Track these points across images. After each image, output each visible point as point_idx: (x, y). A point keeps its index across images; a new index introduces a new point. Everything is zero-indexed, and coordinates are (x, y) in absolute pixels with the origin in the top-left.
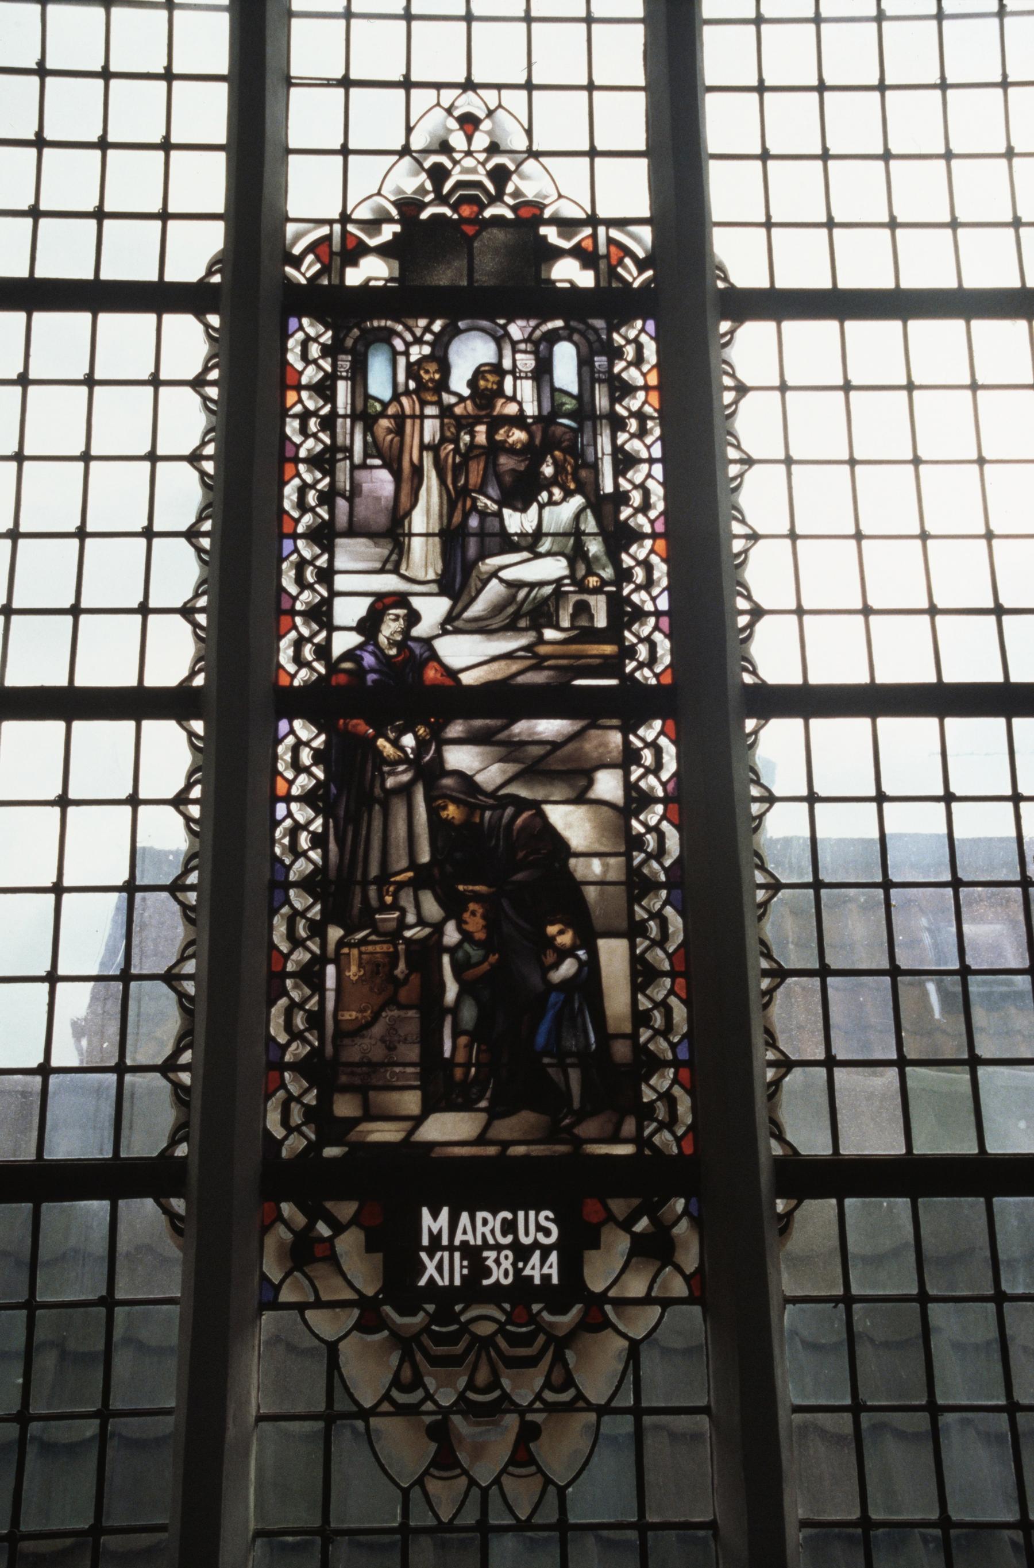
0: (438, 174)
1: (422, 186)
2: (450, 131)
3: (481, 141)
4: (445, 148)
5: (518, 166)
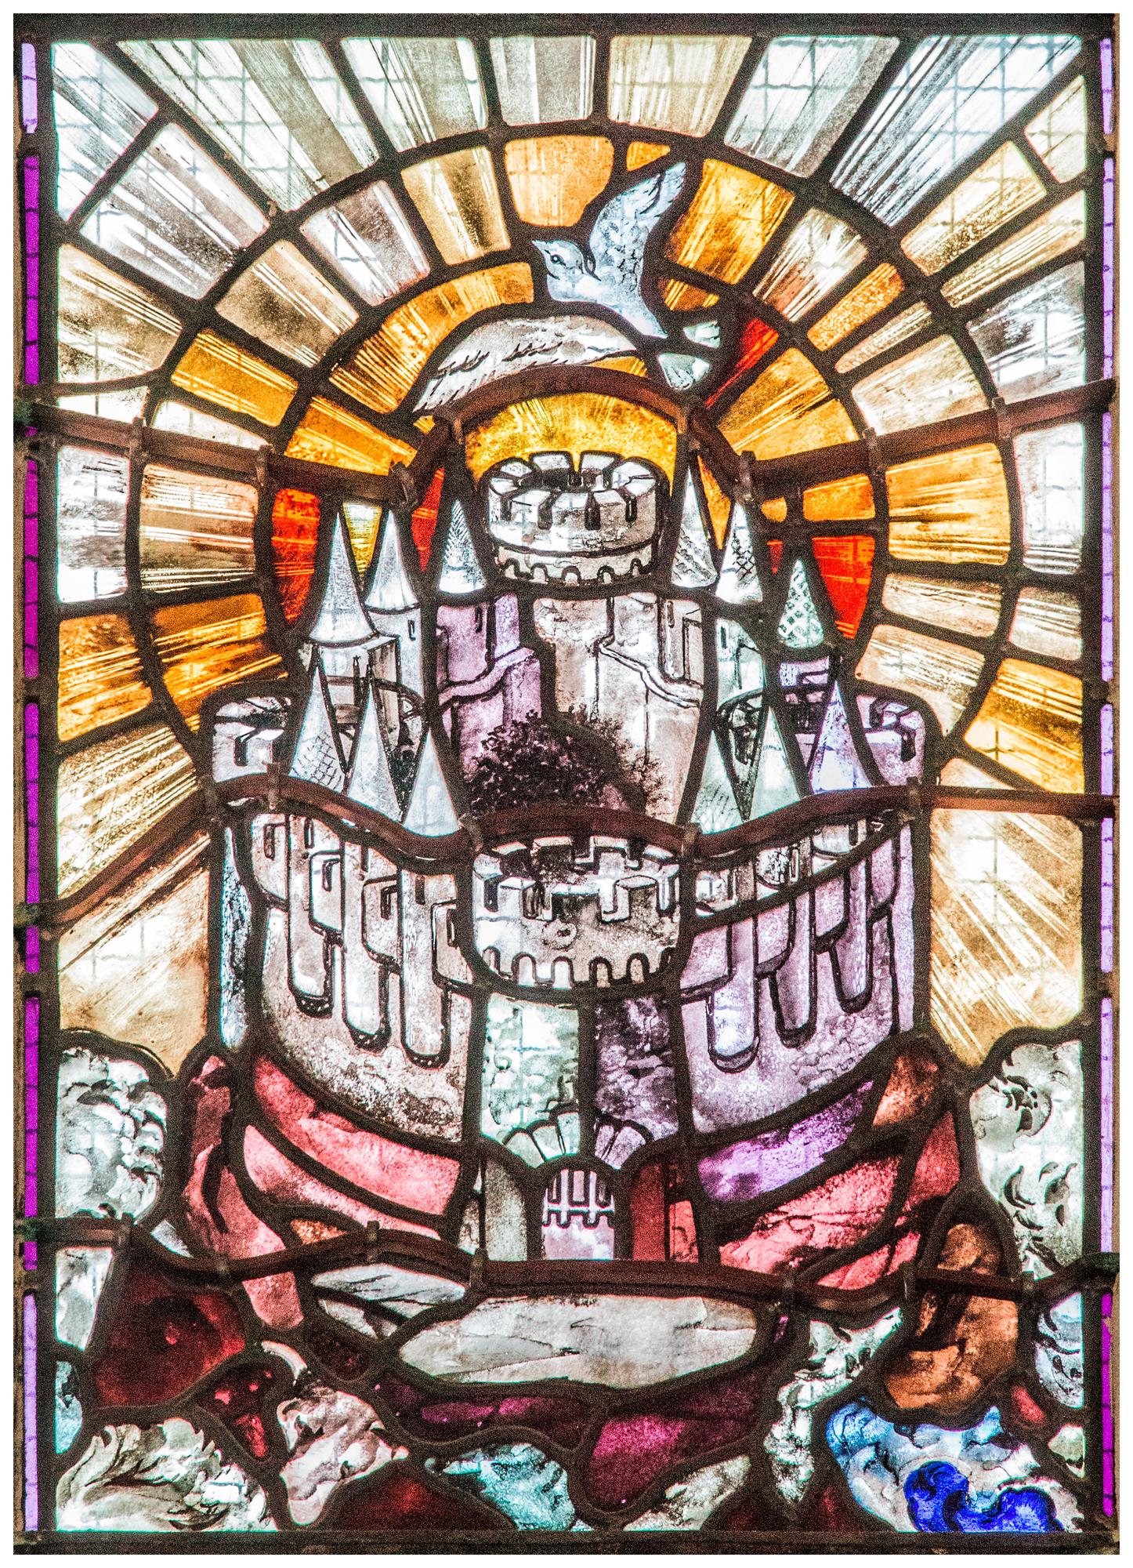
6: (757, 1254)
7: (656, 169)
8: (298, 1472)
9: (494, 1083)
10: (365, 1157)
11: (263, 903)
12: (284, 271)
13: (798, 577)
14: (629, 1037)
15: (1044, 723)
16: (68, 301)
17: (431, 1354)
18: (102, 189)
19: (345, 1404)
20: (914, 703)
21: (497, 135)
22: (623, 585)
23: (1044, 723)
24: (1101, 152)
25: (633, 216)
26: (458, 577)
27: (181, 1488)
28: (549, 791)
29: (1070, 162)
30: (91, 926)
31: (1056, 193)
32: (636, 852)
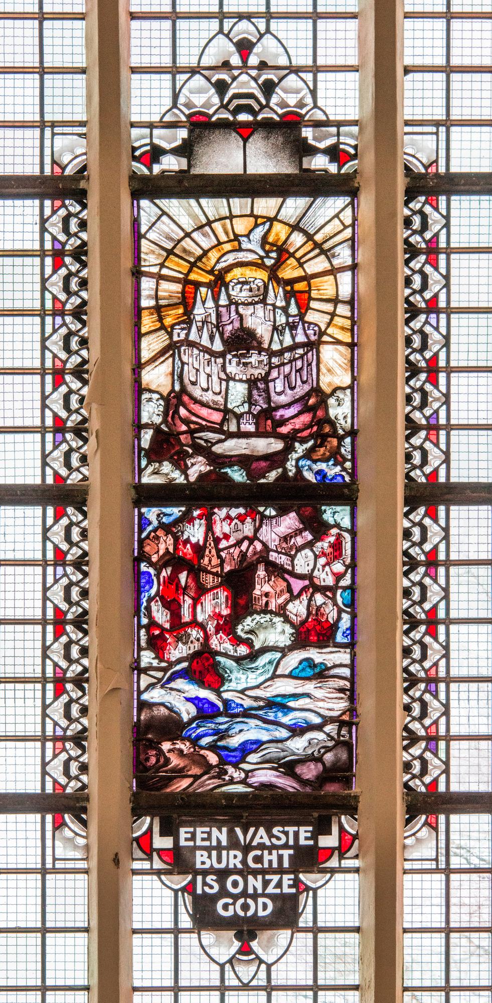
0: (221, 87)
1: (210, 98)
2: (231, 55)
3: (253, 60)
4: (226, 65)
5: (281, 80)
6: (284, 430)
7: (264, 223)
8: (190, 472)
9: (230, 398)
10: (204, 412)
11: (183, 363)
12: (187, 243)
13: (293, 301)
14: (258, 389)
15: (343, 328)
16: (143, 249)
17: (218, 449)
18: (150, 228)
19: (200, 458)
20: (316, 325)
21: (231, 217)
22: (257, 303)
23: (343, 328)
24: (355, 219)
25: (259, 232)
26: (223, 301)
27: (167, 475)
28: (242, 342)
29: (348, 221)
30: (148, 368)
31: (345, 227)
32: (260, 354)
